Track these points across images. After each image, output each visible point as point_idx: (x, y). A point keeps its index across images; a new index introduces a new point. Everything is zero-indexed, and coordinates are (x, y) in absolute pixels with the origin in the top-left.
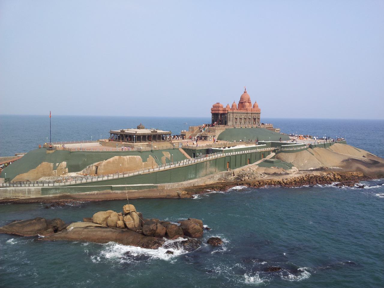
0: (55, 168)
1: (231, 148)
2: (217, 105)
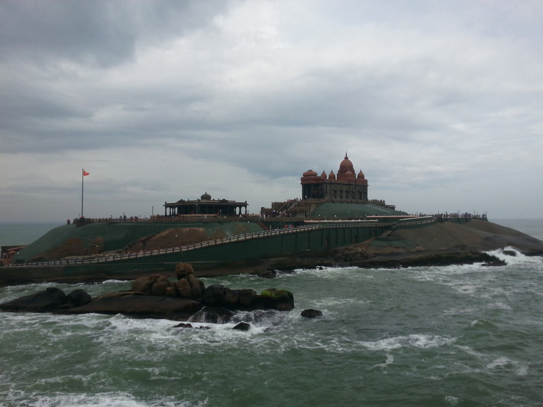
2: (309, 172)
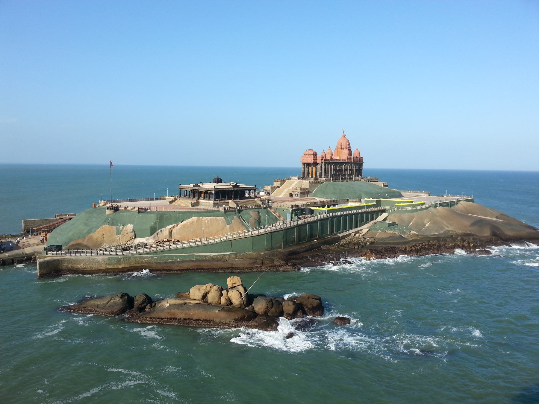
0: (118, 233)
1: (331, 208)
